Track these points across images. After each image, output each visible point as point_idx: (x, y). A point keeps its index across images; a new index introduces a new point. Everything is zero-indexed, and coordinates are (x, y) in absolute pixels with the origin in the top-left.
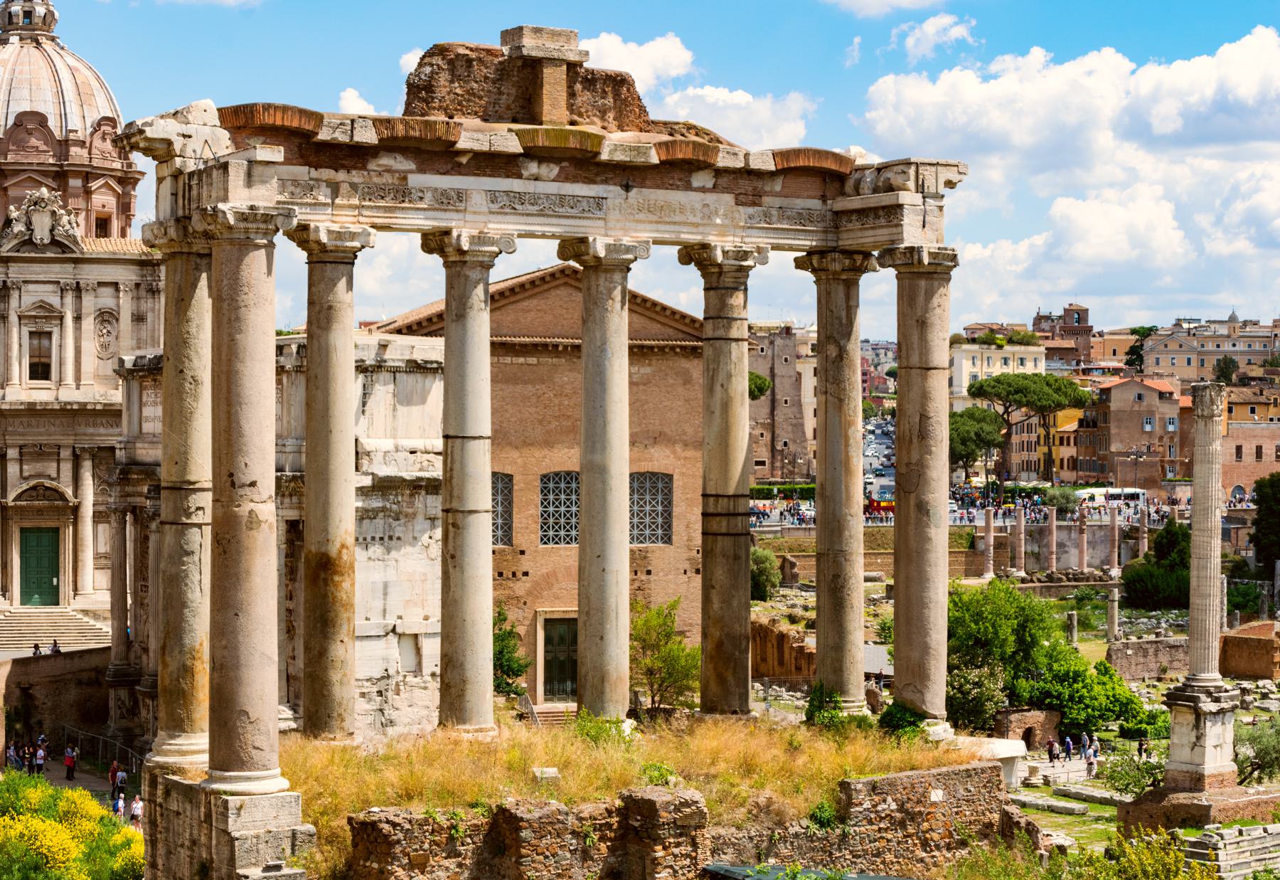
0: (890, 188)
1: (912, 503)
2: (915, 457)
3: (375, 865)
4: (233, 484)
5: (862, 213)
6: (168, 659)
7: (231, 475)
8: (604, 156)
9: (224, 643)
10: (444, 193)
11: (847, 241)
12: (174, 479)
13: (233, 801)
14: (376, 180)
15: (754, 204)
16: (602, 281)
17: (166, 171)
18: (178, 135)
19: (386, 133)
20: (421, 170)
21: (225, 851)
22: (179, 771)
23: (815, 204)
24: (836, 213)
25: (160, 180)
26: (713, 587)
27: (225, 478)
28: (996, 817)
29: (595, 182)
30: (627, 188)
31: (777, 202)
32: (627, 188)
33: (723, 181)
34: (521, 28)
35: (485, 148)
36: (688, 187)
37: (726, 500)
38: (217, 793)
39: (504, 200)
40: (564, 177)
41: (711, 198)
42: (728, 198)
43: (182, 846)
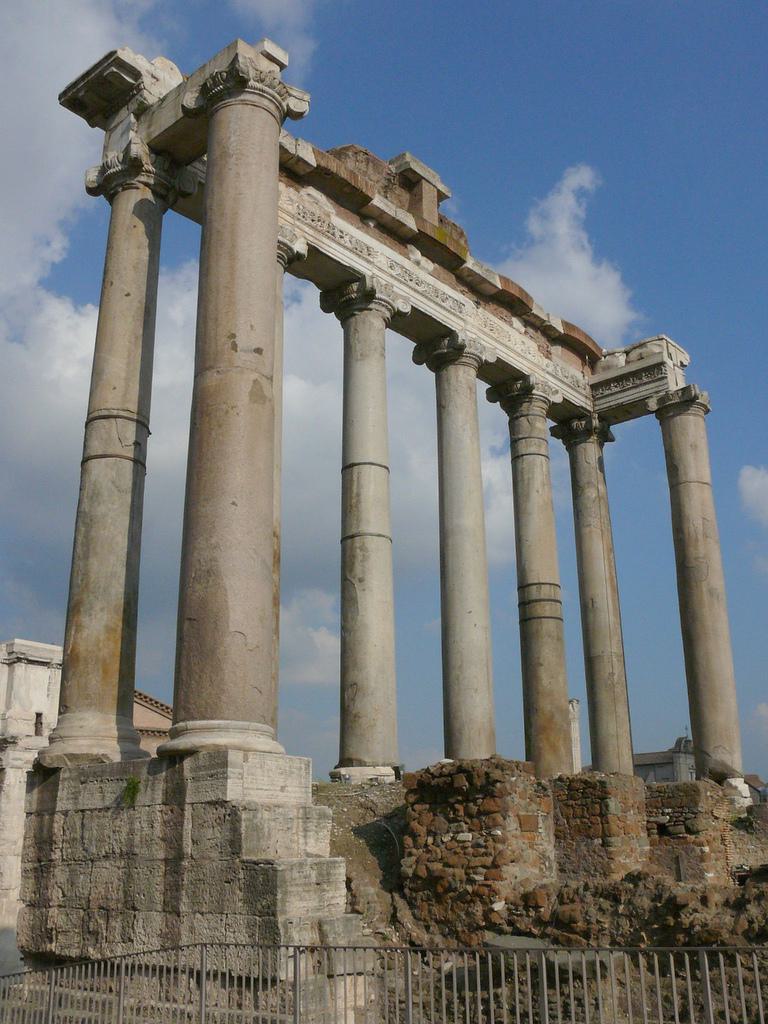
1: (704, 589)
3: (467, 836)
4: (234, 347)
5: (619, 379)
7: (233, 336)
9: (213, 541)
10: (357, 242)
12: (109, 406)
13: (234, 757)
14: (307, 205)
15: (547, 357)
16: (461, 373)
18: (148, 72)
19: (323, 164)
20: (337, 215)
21: (215, 835)
23: (579, 376)
24: (594, 387)
26: (541, 665)
27: (224, 339)
29: (454, 288)
31: (561, 363)
36: (511, 325)
37: (548, 586)
39: (398, 271)
41: (526, 339)
42: (532, 346)
43: (106, 857)
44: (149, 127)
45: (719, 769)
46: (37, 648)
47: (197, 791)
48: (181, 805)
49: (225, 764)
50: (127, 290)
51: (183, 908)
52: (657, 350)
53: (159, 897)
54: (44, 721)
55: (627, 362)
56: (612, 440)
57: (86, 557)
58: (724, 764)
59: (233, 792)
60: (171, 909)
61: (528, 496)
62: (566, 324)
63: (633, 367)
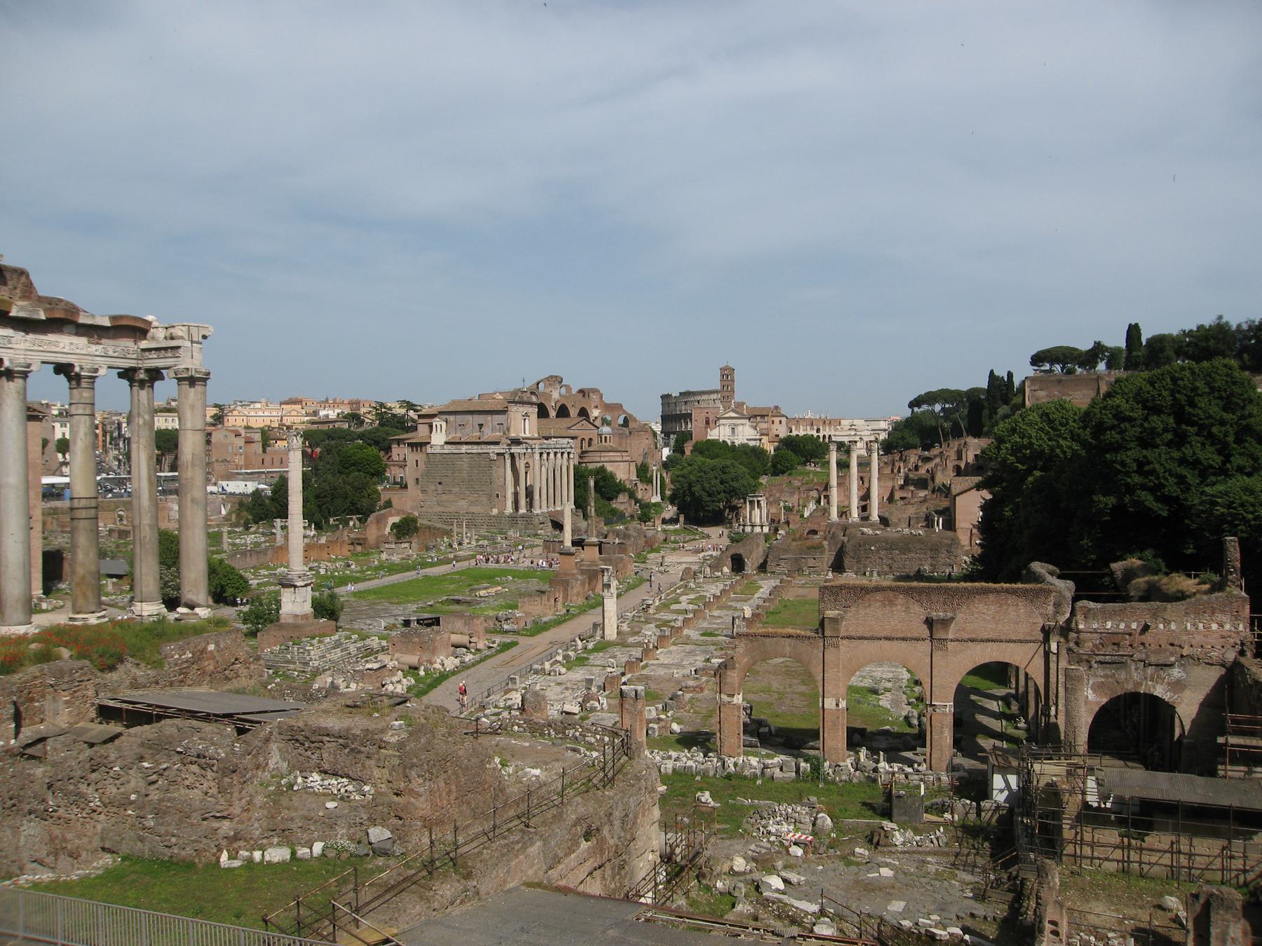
2: (189, 474)
8: (13, 313)
24: (143, 350)
42: (83, 341)
52: (180, 334)
55: (166, 338)
56: (163, 379)
62: (113, 318)
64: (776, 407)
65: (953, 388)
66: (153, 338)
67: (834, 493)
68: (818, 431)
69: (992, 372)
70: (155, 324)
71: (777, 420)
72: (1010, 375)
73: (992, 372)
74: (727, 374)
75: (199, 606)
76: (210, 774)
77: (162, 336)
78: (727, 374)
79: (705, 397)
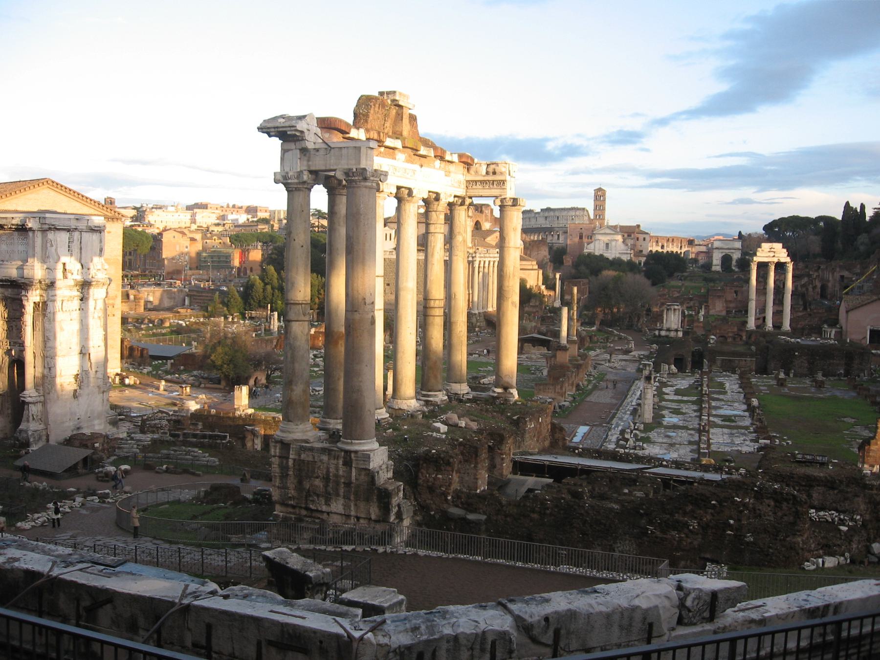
0: (494, 173)
3: (440, 476)
4: (365, 303)
5: (482, 182)
6: (294, 388)
11: (471, 193)
17: (292, 146)
22: (307, 441)
24: (467, 181)
25: (284, 151)
28: (549, 427)
30: (422, 166)
32: (422, 166)
33: (443, 163)
34: (394, 92)
35: (392, 145)
36: (434, 167)
38: (356, 452)
40: (407, 161)
42: (442, 173)
43: (317, 477)
44: (308, 161)
45: (506, 385)
46: (59, 219)
47: (357, 464)
48: (351, 467)
49: (369, 458)
50: (301, 244)
51: (352, 498)
52: (503, 170)
53: (342, 494)
54: (67, 267)
55: (487, 173)
57: (293, 362)
58: (508, 383)
59: (372, 466)
60: (346, 497)
61: (433, 255)
63: (491, 178)
64: (638, 226)
65: (802, 215)
66: (476, 172)
67: (752, 306)
68: (663, 247)
69: (847, 204)
70: (476, 161)
71: (641, 237)
72: (863, 207)
73: (847, 204)
74: (600, 196)
75: (512, 387)
76: (785, 505)
77: (484, 172)
78: (600, 196)
79: (564, 213)
